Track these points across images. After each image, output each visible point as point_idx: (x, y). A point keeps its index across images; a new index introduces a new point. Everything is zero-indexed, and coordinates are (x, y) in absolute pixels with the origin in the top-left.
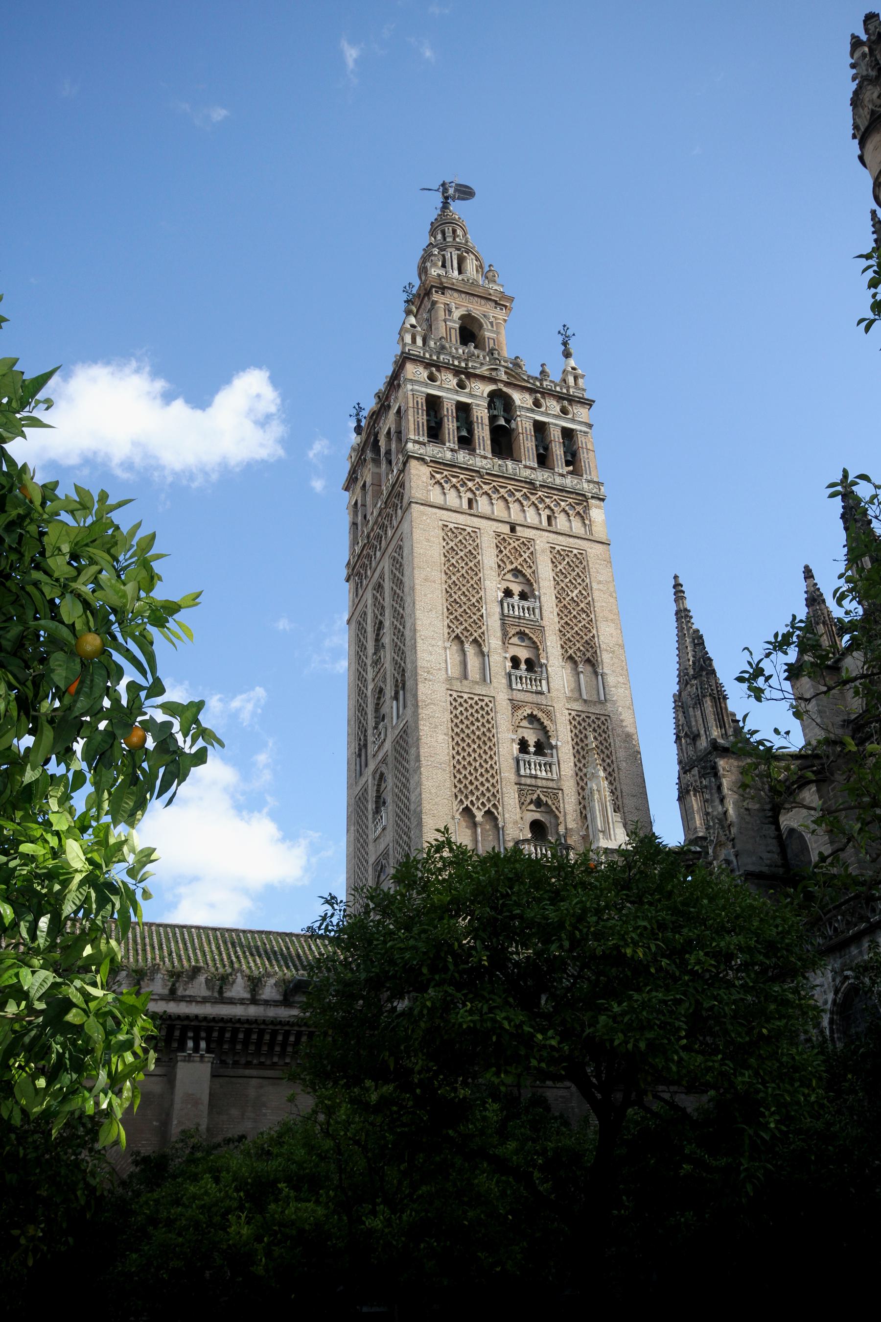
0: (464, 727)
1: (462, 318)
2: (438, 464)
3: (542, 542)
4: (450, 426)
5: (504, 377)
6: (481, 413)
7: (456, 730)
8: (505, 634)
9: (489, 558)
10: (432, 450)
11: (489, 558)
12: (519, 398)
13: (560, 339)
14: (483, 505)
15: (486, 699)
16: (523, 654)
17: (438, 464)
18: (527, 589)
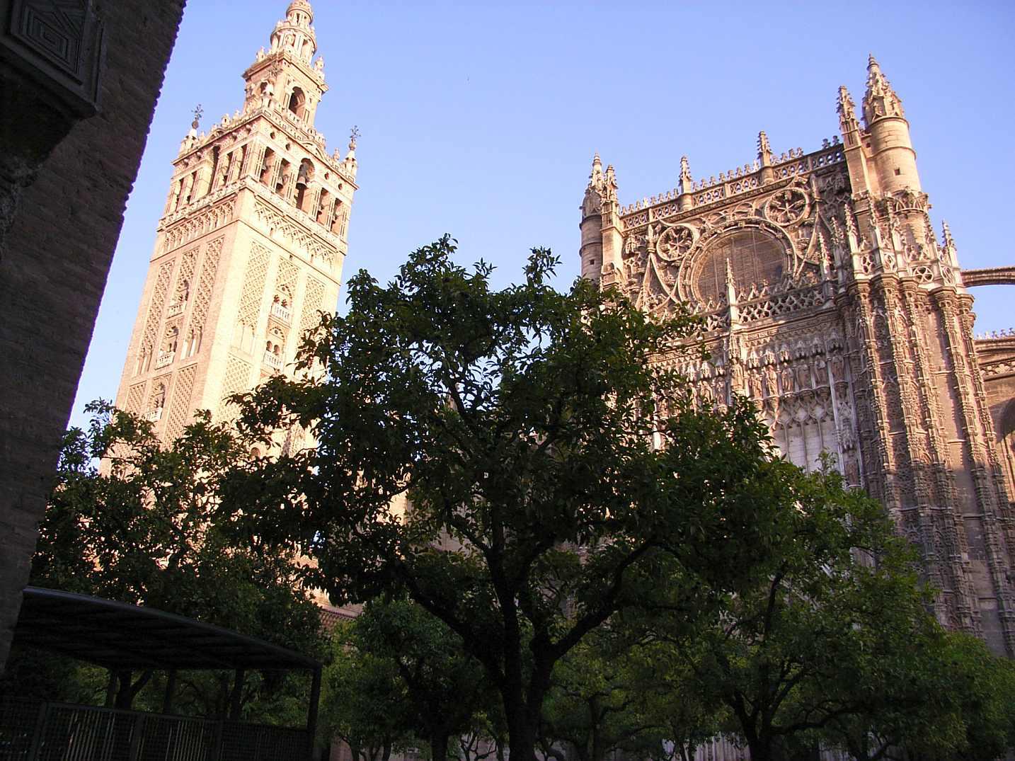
0: (231, 379)
1: (295, 88)
2: (261, 199)
3: (305, 271)
4: (273, 174)
5: (314, 152)
6: (294, 169)
7: (228, 380)
8: (269, 324)
9: (272, 272)
10: (258, 188)
11: (272, 272)
12: (319, 169)
13: (352, 134)
14: (278, 236)
15: (248, 365)
16: (275, 341)
17: (261, 199)
18: (288, 299)
